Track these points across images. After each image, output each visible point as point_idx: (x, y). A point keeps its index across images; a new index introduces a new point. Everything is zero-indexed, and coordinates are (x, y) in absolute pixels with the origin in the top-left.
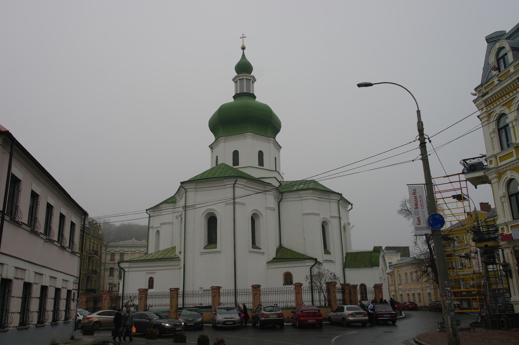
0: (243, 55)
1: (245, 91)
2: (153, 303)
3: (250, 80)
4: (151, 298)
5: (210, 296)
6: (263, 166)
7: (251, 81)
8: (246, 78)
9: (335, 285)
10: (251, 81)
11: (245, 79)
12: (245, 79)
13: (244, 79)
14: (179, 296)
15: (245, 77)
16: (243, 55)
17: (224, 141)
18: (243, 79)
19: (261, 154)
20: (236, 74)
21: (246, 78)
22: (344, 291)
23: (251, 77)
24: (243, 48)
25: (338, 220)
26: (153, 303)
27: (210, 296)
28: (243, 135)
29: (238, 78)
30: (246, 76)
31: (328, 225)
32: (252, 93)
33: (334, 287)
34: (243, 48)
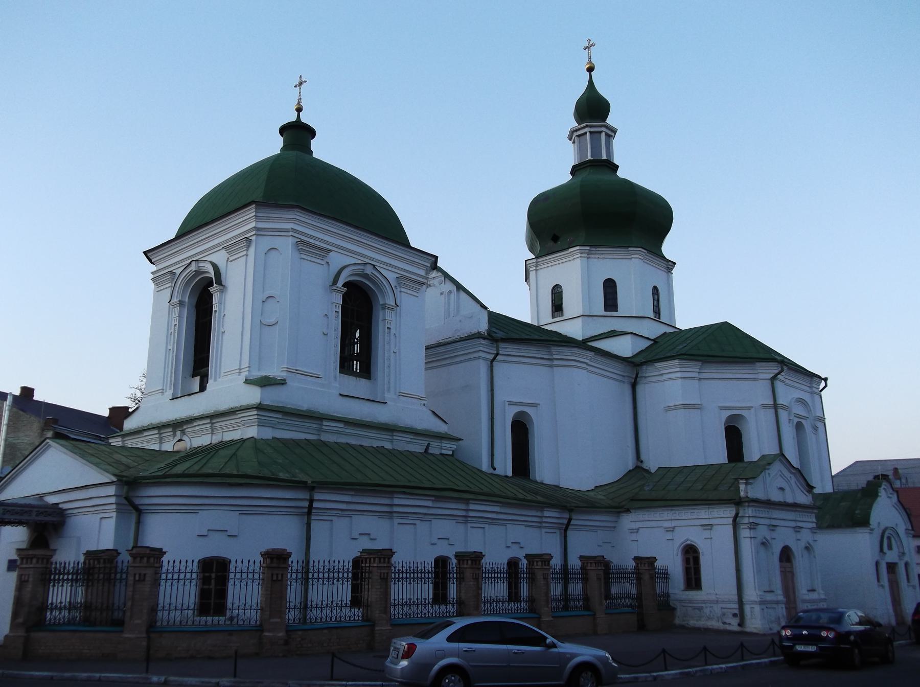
1: (589, 158)
2: (408, 588)
3: (601, 132)
4: (318, 578)
5: (191, 579)
6: (617, 311)
7: (603, 135)
8: (591, 132)
9: (549, 562)
10: (603, 135)
13: (586, 133)
14: (311, 575)
17: (535, 268)
20: (575, 124)
21: (591, 132)
22: (533, 574)
23: (601, 126)
25: (773, 411)
26: (408, 588)
27: (253, 579)
29: (575, 134)
30: (591, 127)
31: (804, 427)
32: (604, 157)
33: (380, 562)
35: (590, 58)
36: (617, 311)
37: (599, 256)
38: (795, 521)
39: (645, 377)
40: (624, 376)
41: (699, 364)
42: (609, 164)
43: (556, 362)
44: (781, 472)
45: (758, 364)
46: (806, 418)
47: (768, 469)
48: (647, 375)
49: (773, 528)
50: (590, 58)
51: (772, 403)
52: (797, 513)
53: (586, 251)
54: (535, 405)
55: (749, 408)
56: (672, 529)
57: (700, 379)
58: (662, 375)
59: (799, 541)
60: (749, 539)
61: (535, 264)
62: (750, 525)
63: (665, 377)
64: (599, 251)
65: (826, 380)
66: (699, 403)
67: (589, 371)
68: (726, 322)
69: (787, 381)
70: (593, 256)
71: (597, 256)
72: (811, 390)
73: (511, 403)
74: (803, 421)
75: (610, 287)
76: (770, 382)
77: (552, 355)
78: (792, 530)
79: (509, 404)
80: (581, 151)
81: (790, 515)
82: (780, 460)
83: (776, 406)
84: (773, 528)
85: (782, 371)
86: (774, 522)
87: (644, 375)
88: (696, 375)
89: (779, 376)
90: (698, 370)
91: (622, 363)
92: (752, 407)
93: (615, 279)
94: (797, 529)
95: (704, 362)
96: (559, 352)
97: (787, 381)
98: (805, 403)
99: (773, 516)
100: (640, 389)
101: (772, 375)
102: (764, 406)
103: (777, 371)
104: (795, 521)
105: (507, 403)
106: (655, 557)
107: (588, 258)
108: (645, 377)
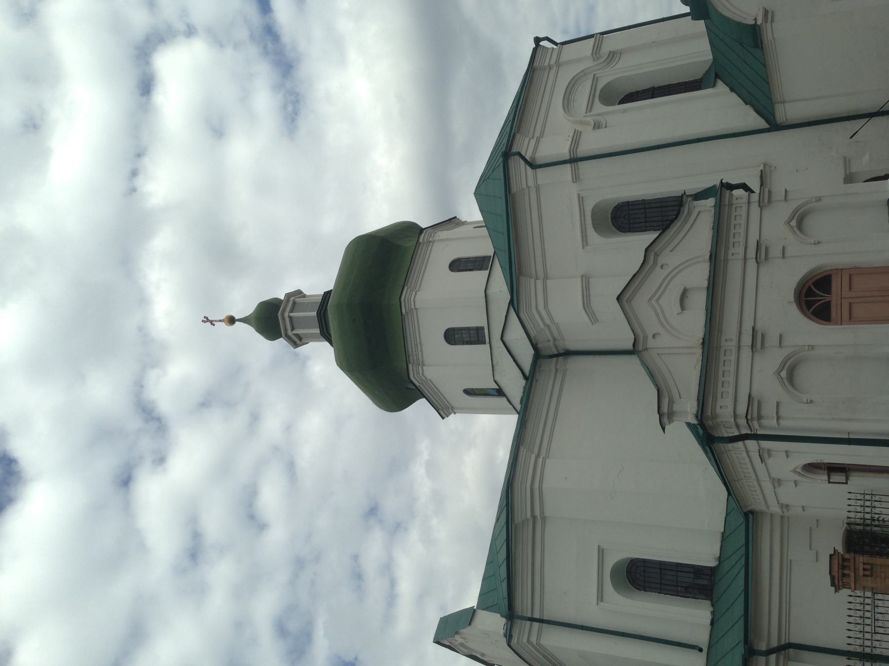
0: (244, 320)
1: (318, 331)
8: (293, 329)
11: (294, 332)
12: (294, 332)
15: (290, 333)
16: (244, 320)
18: (294, 334)
19: (457, 265)
24: (231, 320)
25: (581, 164)
28: (421, 386)
30: (286, 330)
32: (315, 314)
34: (231, 320)
35: (220, 321)
36: (482, 328)
37: (419, 349)
38: (745, 259)
39: (555, 340)
40: (557, 370)
41: (522, 279)
42: (323, 306)
43: (537, 513)
44: (650, 299)
45: (514, 189)
46: (595, 80)
47: (645, 338)
48: (552, 340)
49: (758, 341)
50: (220, 321)
51: (568, 165)
52: (730, 257)
53: (415, 369)
54: (601, 552)
55: (581, 199)
56: (777, 482)
57: (546, 277)
58: (548, 326)
59: (788, 253)
60: (780, 421)
61: (445, 411)
62: (752, 419)
63: (548, 321)
64: (412, 352)
65: (537, 40)
66: (579, 280)
67: (547, 456)
68: (476, 194)
69: (537, 134)
70: (420, 357)
71: (420, 352)
72: (555, 68)
73: (600, 598)
74: (600, 86)
75: (453, 336)
76: (539, 171)
77: (528, 519)
78: (766, 213)
79: (602, 601)
80: (313, 338)
81: (735, 268)
82: (629, 301)
83: (574, 160)
84: (758, 341)
85: (519, 154)
86: (747, 340)
87: (551, 343)
88: (540, 283)
89: (527, 157)
90: (532, 281)
91: (537, 380)
92: (579, 195)
93: (445, 330)
94: (762, 254)
95: (520, 273)
96: (522, 513)
97: (537, 134)
98: (571, 85)
99: (734, 343)
100: (573, 347)
101: (528, 168)
102: (576, 178)
103: (522, 162)
104: (745, 259)
105: (601, 604)
106: (831, 555)
107: (423, 365)
108: (555, 340)
